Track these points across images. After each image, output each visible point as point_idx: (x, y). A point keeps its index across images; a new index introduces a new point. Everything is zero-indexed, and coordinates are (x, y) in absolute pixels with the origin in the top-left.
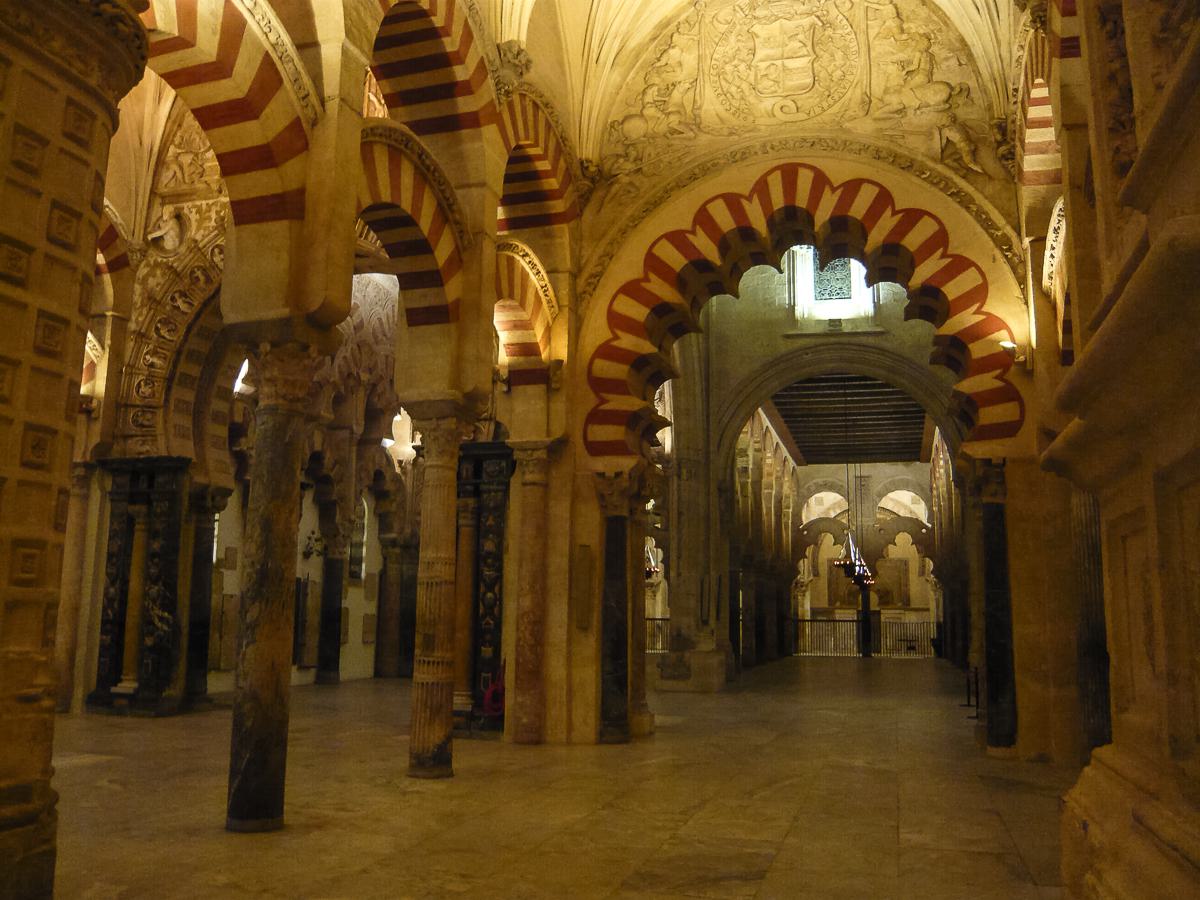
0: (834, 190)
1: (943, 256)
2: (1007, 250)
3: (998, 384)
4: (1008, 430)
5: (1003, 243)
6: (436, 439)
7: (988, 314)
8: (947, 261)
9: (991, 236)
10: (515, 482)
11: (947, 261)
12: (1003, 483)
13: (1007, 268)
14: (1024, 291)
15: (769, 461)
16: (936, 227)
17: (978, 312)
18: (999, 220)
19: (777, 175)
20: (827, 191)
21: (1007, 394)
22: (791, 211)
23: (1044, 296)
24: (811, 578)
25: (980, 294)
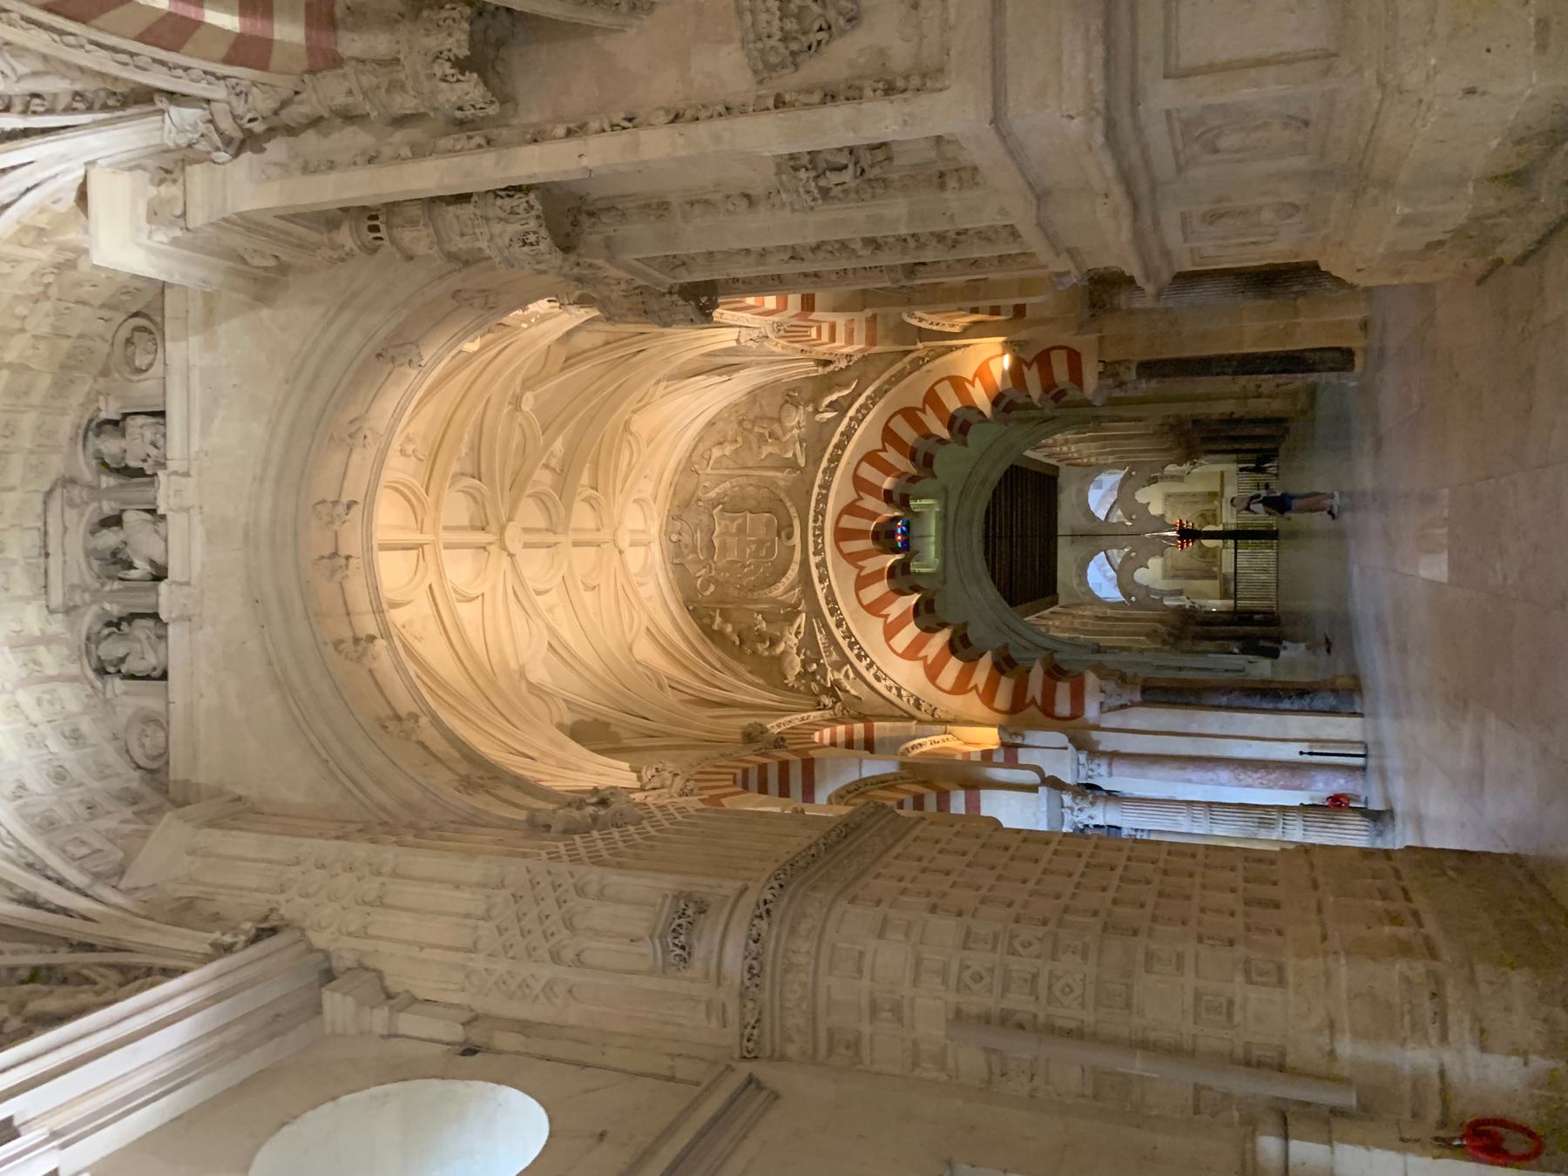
0: (860, 498)
1: (923, 411)
2: (923, 359)
3: (1035, 368)
4: (1074, 359)
5: (917, 364)
6: (1080, 810)
7: (976, 375)
8: (928, 408)
9: (910, 373)
10: (1106, 784)
11: (928, 408)
12: (1118, 362)
13: (938, 361)
14: (958, 348)
15: (1057, 623)
16: (899, 417)
17: (972, 383)
18: (898, 367)
19: (843, 545)
20: (859, 503)
21: (1043, 360)
22: (875, 536)
23: (965, 333)
24: (1184, 597)
25: (958, 383)
